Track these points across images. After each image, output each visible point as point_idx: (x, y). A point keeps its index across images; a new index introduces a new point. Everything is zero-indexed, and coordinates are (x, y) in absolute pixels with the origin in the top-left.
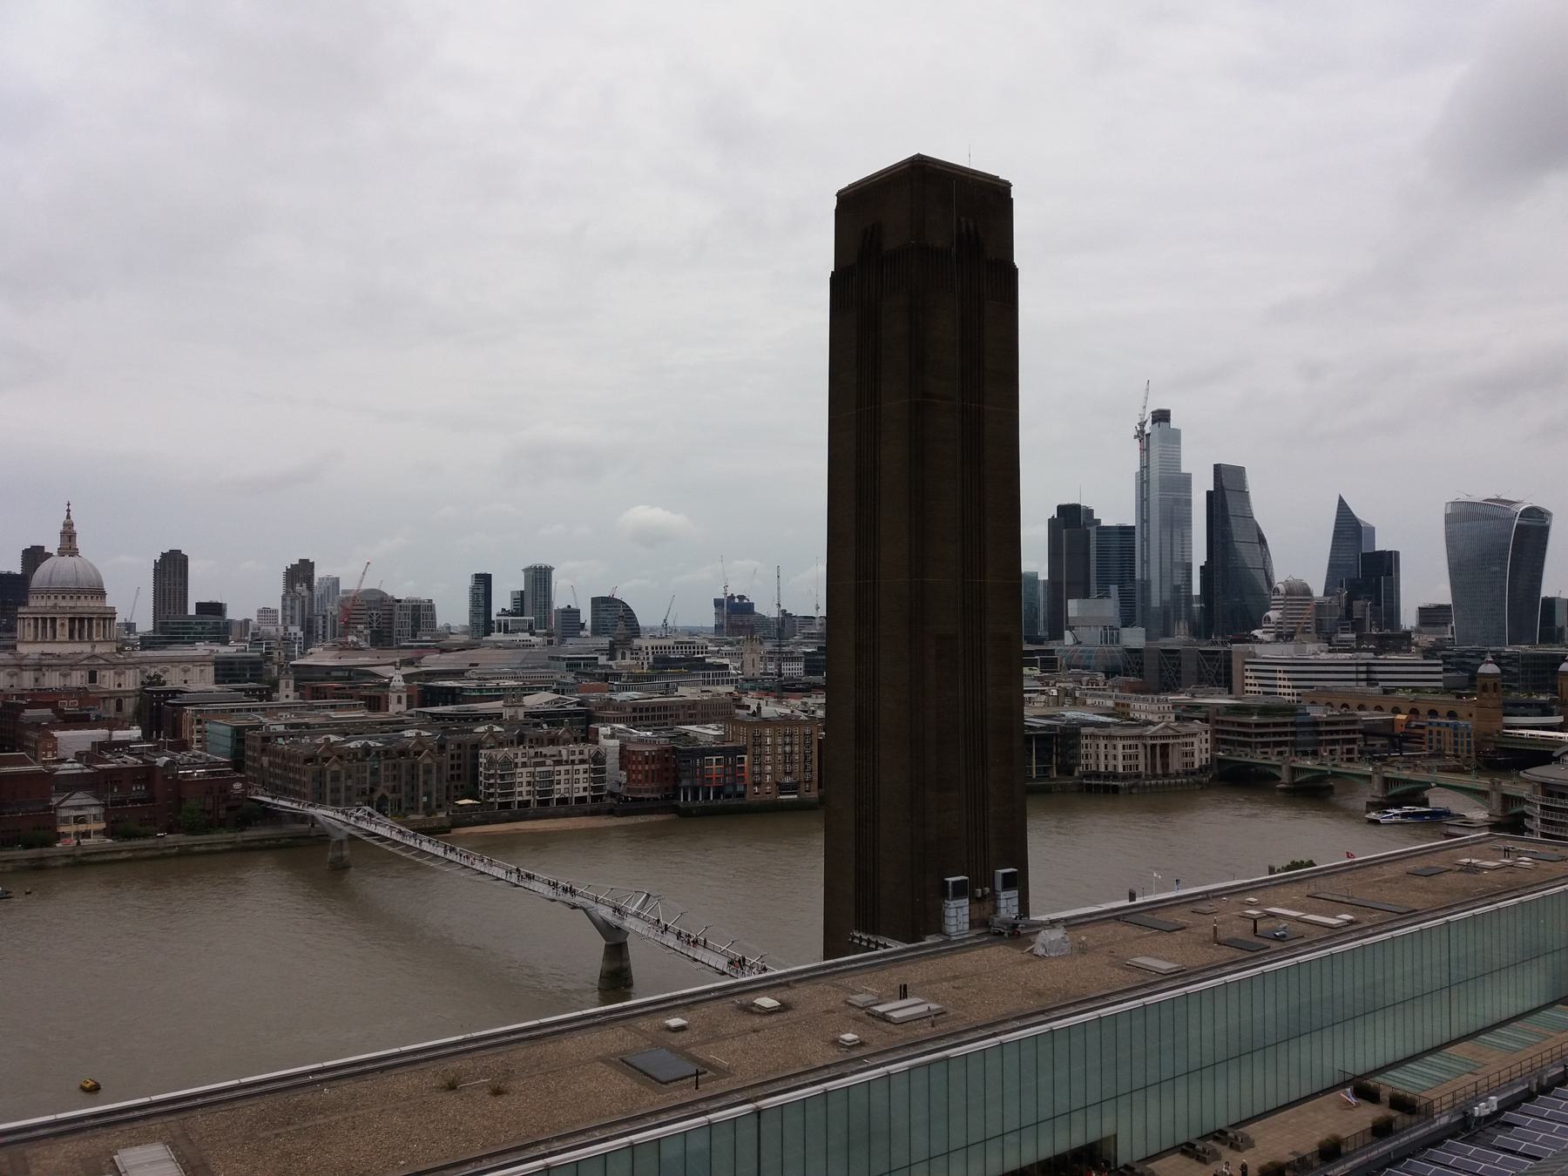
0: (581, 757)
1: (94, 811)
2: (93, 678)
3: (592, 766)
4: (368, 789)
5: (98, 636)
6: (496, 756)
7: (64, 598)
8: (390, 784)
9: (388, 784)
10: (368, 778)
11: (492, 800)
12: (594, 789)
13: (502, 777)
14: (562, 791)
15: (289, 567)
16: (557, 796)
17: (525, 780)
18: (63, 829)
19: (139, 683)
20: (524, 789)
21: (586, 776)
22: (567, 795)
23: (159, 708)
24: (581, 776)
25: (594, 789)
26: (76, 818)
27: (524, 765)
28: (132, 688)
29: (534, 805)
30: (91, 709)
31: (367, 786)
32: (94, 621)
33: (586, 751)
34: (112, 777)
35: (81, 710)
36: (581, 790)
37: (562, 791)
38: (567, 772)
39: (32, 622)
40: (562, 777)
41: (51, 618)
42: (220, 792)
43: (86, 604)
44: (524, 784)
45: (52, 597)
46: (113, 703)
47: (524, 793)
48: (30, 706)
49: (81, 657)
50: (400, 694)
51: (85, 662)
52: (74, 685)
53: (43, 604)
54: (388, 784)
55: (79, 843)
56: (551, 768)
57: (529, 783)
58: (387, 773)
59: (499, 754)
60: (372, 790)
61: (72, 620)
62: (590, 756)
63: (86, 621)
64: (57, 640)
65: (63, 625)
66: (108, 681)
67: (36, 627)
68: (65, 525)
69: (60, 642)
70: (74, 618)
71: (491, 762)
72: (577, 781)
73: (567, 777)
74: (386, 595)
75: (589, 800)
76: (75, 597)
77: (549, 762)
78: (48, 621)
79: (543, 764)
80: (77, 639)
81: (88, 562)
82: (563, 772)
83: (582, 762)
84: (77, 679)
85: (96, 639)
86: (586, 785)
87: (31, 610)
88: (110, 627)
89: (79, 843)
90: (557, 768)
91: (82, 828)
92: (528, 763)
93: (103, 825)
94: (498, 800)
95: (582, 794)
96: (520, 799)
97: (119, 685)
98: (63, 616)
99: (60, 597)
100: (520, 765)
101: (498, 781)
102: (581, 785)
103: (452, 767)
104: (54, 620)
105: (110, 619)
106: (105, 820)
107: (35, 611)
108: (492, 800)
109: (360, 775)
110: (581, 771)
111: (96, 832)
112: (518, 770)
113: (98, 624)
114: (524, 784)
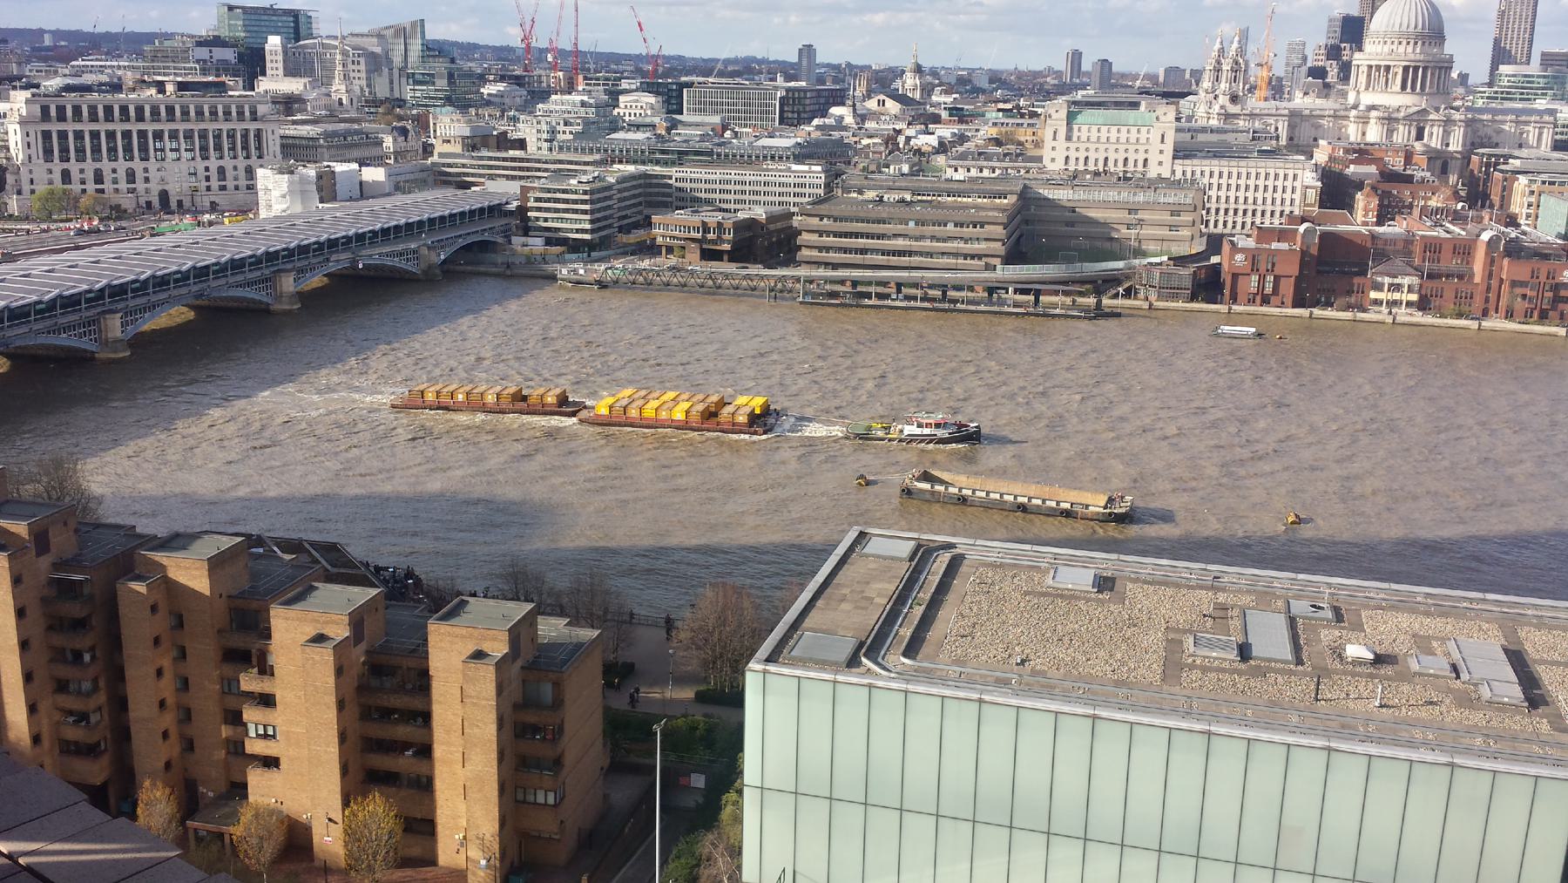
2: (1420, 137)
18: (1373, 295)
19: (1468, 143)
23: (1487, 173)
26: (1391, 285)
28: (1460, 149)
30: (1414, 170)
34: (1433, 247)
35: (1404, 170)
39: (1366, 69)
42: (1548, 278)
46: (1439, 163)
48: (1352, 162)
49: (1411, 110)
51: (1415, 117)
52: (1400, 141)
53: (1379, 50)
55: (1390, 313)
61: (1406, 69)
63: (1421, 70)
64: (1389, 90)
66: (1434, 138)
67: (1369, 75)
80: (1409, 90)
84: (1402, 135)
87: (1367, 57)
89: (1390, 313)
91: (1397, 296)
93: (1414, 297)
97: (1448, 145)
105: (1447, 68)
106: (1419, 292)
107: (1371, 57)
111: (1409, 304)
113: (1432, 74)
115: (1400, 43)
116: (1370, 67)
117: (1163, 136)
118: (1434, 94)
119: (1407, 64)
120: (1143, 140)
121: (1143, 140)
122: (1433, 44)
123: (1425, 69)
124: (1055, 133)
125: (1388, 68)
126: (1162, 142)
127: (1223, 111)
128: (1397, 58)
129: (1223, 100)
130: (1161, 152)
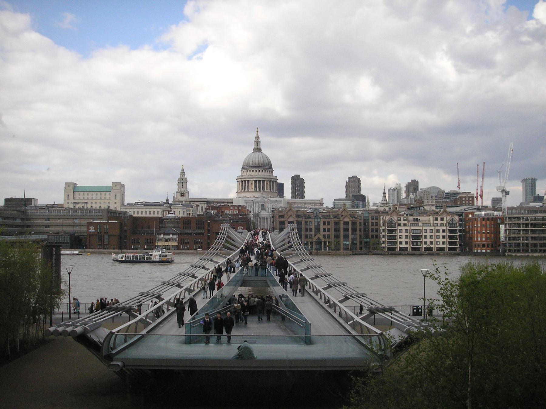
0: (442, 222)
1: (175, 237)
3: (448, 228)
4: (313, 235)
5: (267, 189)
6: (385, 218)
7: (253, 171)
8: (326, 233)
9: (325, 233)
10: (313, 229)
11: (383, 245)
12: (450, 243)
13: (390, 231)
14: (428, 243)
15: (407, 184)
16: (425, 246)
17: (404, 234)
20: (404, 240)
21: (444, 234)
22: (432, 246)
24: (441, 234)
25: (450, 243)
27: (405, 225)
29: (410, 250)
31: (313, 233)
32: (265, 182)
33: (445, 219)
36: (441, 243)
37: (428, 243)
38: (431, 231)
40: (428, 234)
41: (247, 180)
43: (262, 174)
44: (404, 237)
45: (249, 171)
47: (404, 243)
50: (385, 208)
54: (325, 233)
56: (421, 228)
57: (407, 237)
58: (324, 227)
59: (387, 218)
60: (315, 235)
61: (256, 181)
62: (447, 222)
63: (262, 182)
65: (252, 183)
68: (256, 138)
69: (251, 192)
70: (257, 180)
71: (384, 222)
72: (438, 237)
73: (431, 234)
74: (441, 189)
75: (447, 250)
76: (258, 171)
77: (420, 224)
78: (246, 182)
79: (417, 225)
80: (258, 190)
81: (265, 156)
82: (428, 231)
83: (442, 225)
85: (265, 190)
86: (444, 240)
88: (273, 186)
90: (425, 228)
91: (167, 244)
92: (407, 225)
93: (176, 244)
94: (387, 246)
95: (441, 246)
96: (401, 246)
98: (252, 179)
99: (251, 171)
100: (402, 225)
101: (387, 234)
102: (441, 240)
103: (373, 231)
104: (248, 181)
105: (273, 181)
108: (383, 245)
109: (308, 227)
110: (441, 231)
112: (400, 228)
113: (267, 184)
114: (404, 237)
115: (253, 171)
116: (242, 181)
117: (116, 195)
118: (269, 192)
119: (256, 179)
120: (107, 198)
121: (107, 198)
122: (266, 171)
123: (264, 181)
124: (68, 195)
125: (248, 181)
126: (115, 199)
127: (178, 200)
128: (252, 177)
129: (179, 195)
130: (115, 203)
